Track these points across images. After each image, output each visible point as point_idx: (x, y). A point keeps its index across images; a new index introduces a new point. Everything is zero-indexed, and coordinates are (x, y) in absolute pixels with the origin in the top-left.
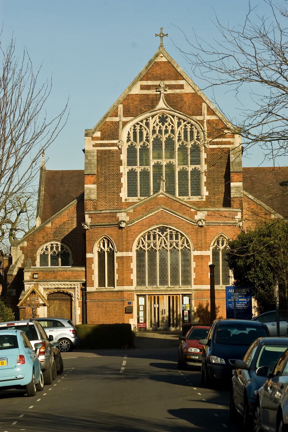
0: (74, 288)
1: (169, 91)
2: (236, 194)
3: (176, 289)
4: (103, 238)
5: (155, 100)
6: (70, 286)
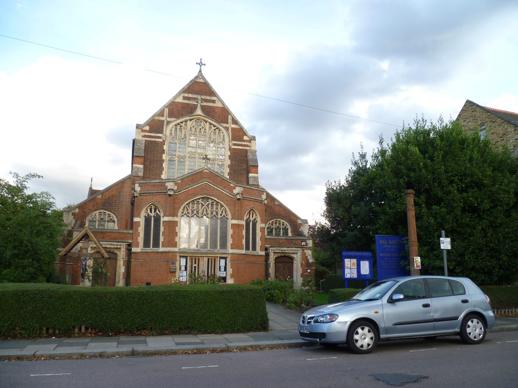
0: (120, 248)
1: (205, 104)
3: (215, 252)
4: (150, 205)
5: (193, 109)
6: (116, 247)
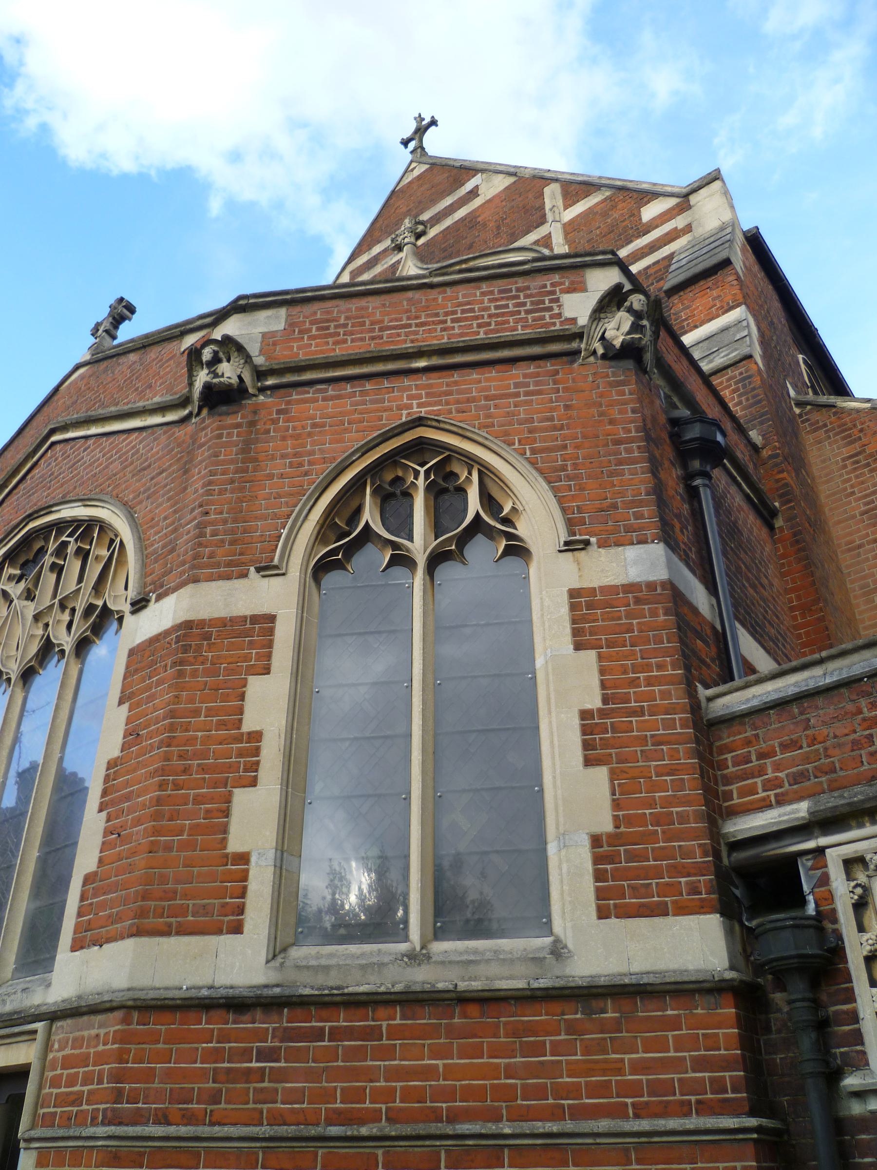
1: (432, 232)
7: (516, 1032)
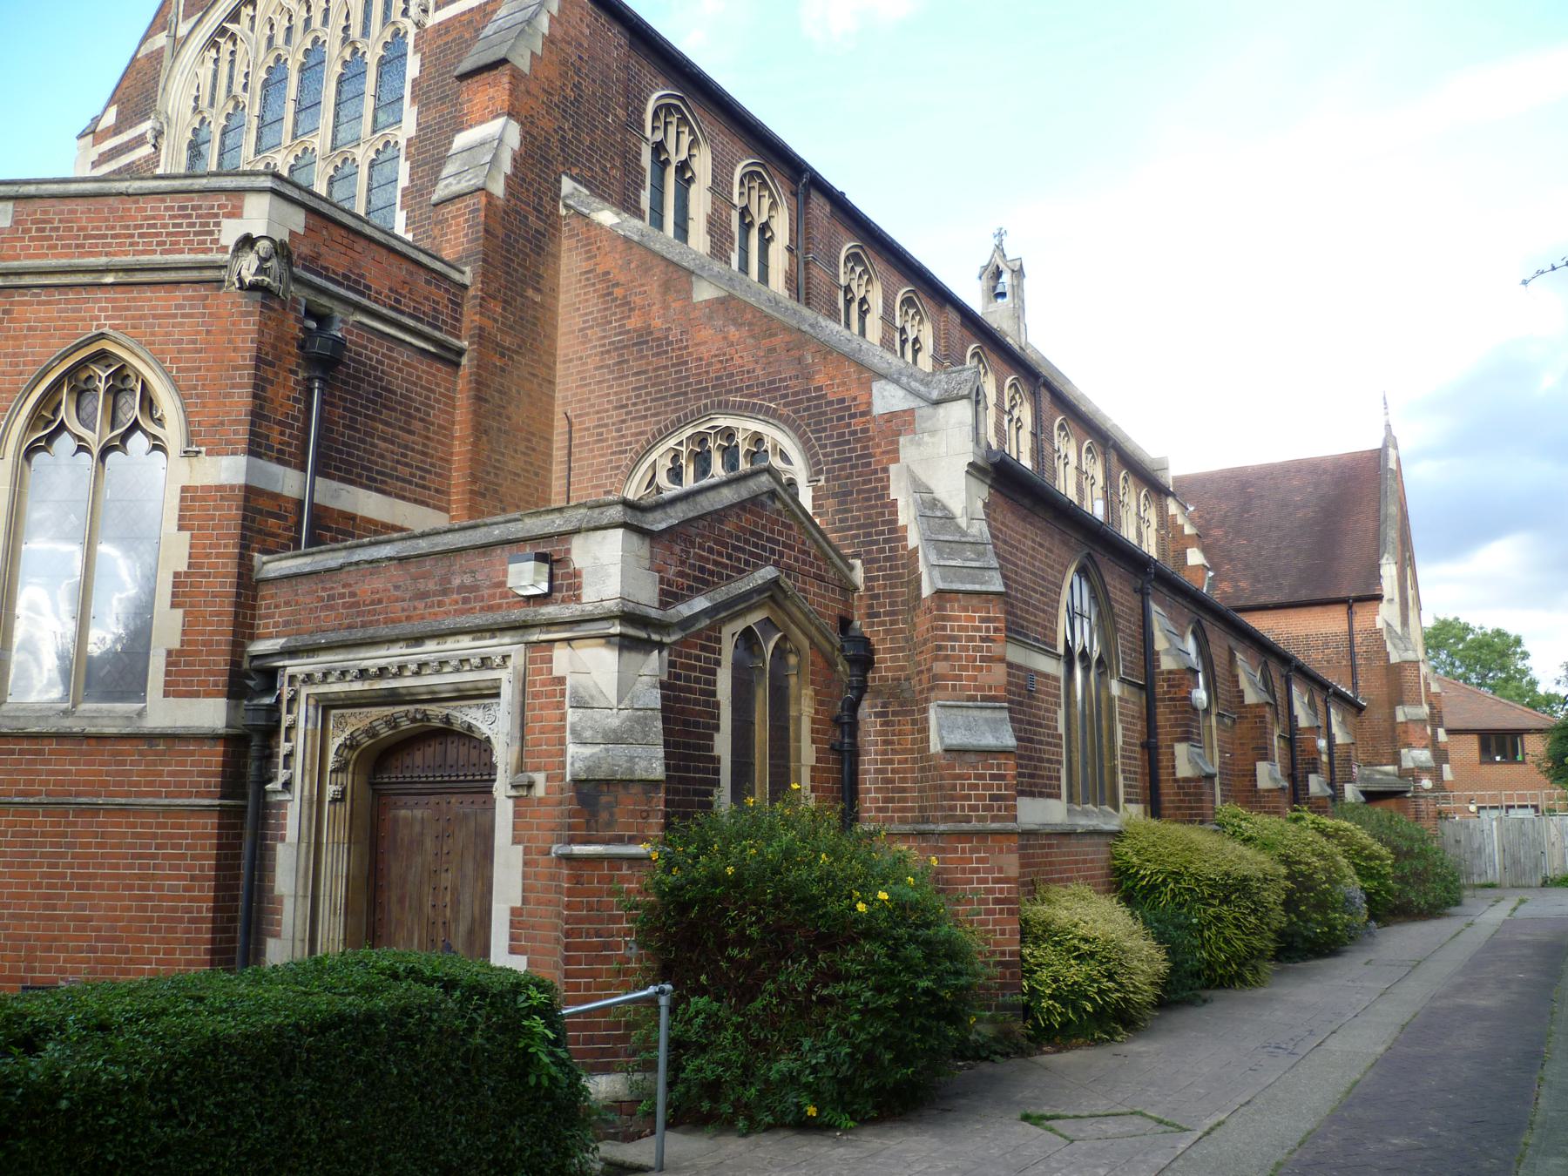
2: (459, 182)
7: (115, 753)
